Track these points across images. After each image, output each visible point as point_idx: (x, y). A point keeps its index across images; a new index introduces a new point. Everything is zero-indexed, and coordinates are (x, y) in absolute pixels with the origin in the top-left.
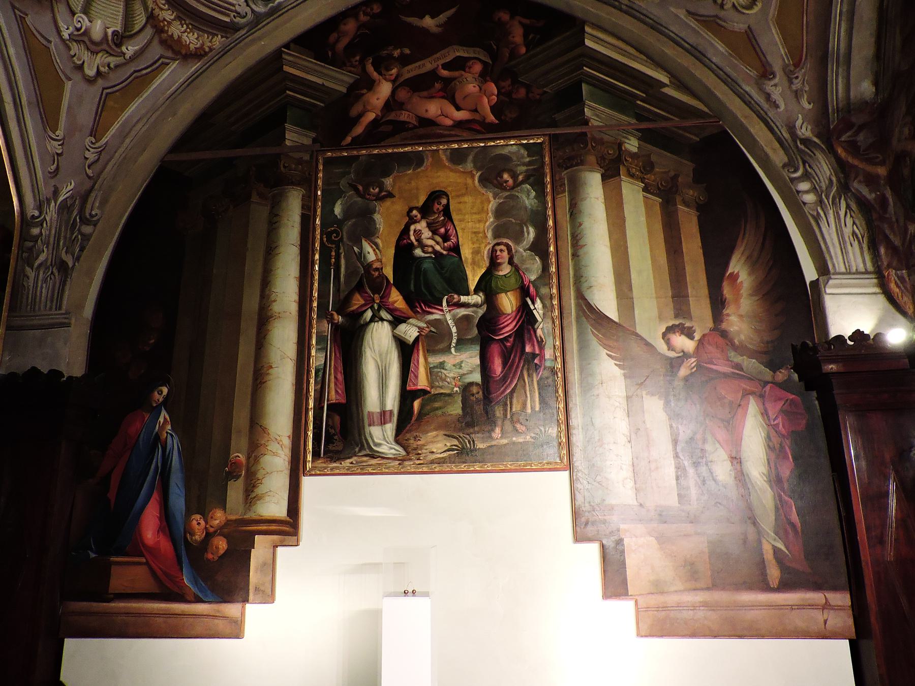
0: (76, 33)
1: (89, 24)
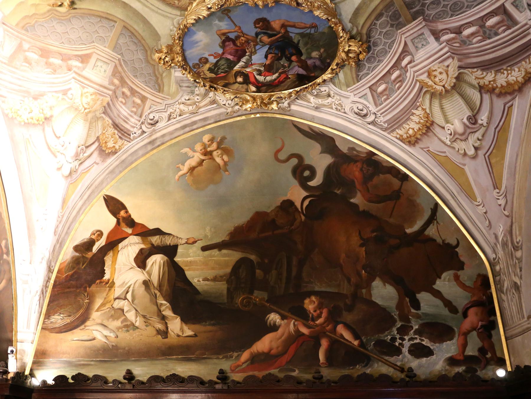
0: (451, 137)
1: (452, 127)
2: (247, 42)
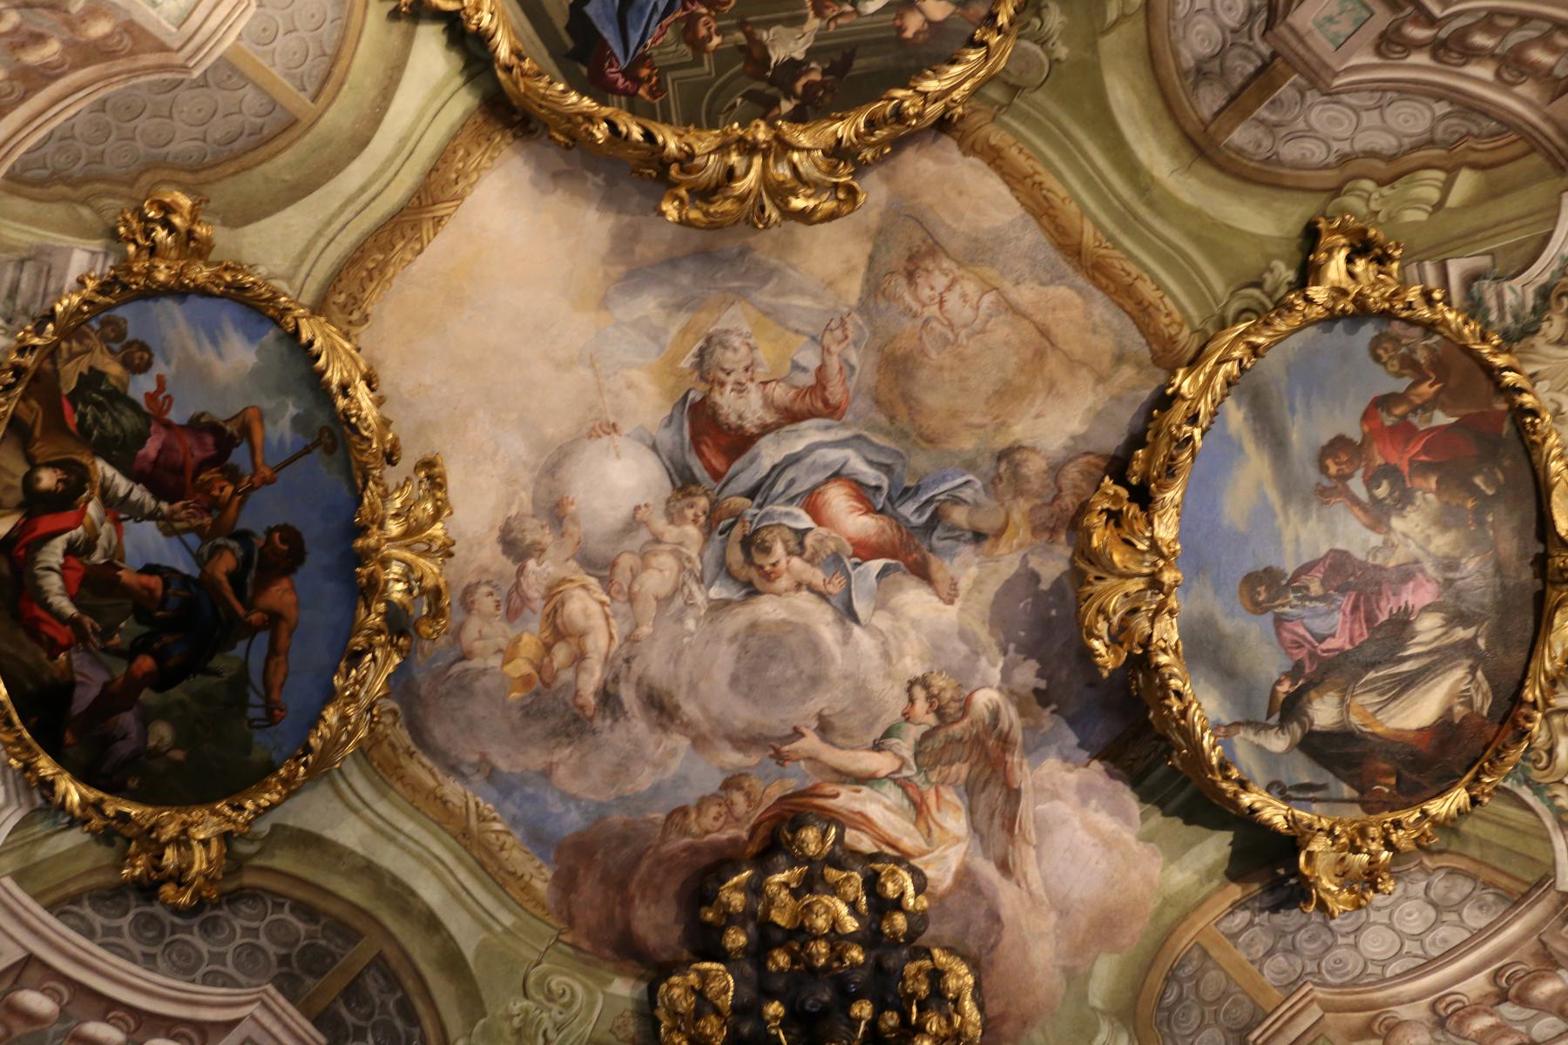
2: (215, 506)
